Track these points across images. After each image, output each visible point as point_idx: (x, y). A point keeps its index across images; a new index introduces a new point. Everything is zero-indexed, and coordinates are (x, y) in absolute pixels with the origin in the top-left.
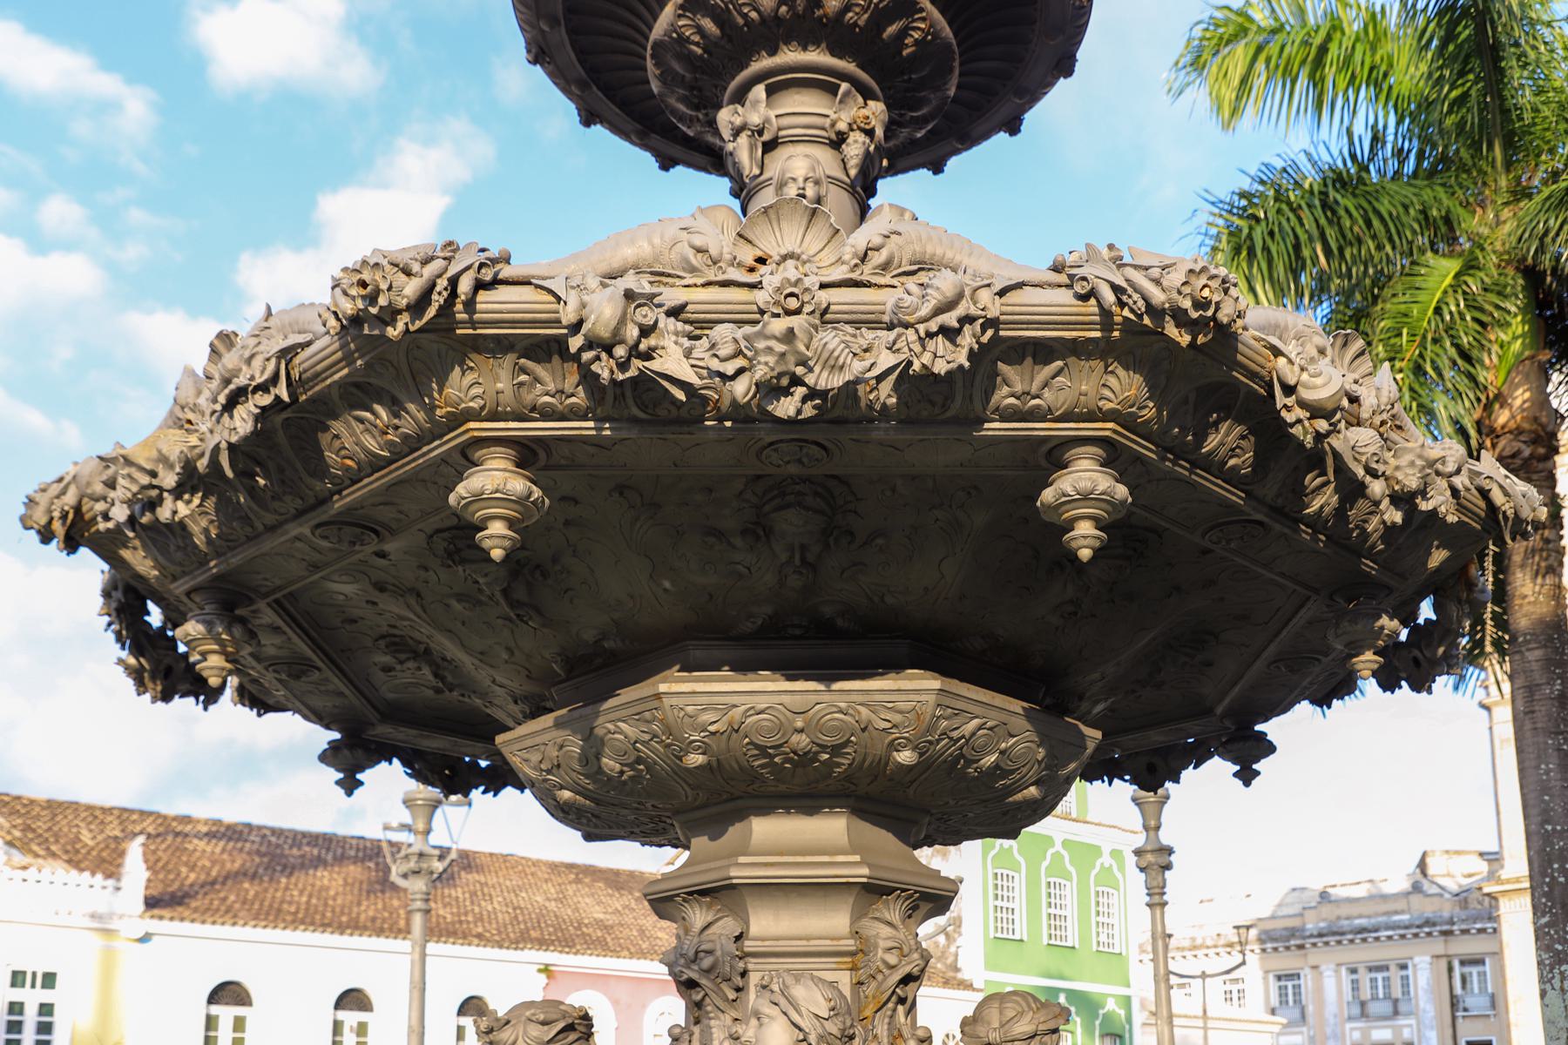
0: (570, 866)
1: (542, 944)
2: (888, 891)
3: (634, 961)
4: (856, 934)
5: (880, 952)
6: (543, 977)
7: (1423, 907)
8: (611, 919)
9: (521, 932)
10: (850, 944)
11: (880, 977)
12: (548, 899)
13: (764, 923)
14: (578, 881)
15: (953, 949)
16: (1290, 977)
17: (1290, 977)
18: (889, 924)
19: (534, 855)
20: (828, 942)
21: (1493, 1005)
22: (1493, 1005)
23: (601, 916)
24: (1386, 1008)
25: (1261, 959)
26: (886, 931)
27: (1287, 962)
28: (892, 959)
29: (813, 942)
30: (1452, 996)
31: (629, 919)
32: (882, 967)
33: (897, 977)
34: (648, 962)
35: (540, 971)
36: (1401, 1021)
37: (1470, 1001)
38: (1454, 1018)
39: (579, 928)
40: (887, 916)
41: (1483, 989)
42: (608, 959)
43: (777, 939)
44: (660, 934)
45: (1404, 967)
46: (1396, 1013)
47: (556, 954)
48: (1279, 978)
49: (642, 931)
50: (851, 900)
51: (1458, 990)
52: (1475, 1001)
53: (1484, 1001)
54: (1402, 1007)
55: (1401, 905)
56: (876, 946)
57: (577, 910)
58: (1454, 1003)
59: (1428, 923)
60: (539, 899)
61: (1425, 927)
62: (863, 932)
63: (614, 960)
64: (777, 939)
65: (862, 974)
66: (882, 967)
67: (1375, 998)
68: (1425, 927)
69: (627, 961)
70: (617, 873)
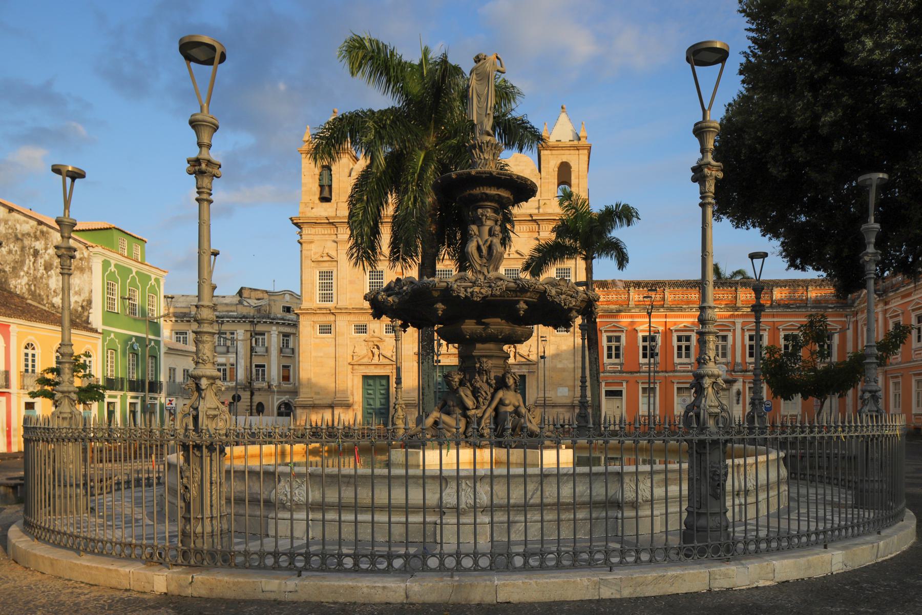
7: (243, 310)
15: (86, 314)
16: (182, 333)
17: (182, 333)
21: (267, 351)
22: (267, 351)
24: (224, 349)
25: (173, 325)
27: (182, 327)
30: (251, 347)
36: (230, 355)
37: (258, 349)
38: (251, 355)
41: (263, 345)
45: (233, 334)
46: (228, 352)
48: (177, 333)
51: (254, 345)
52: (260, 349)
53: (263, 349)
54: (231, 350)
55: (234, 308)
58: (252, 349)
59: (244, 317)
61: (242, 319)
67: (219, 345)
68: (242, 319)
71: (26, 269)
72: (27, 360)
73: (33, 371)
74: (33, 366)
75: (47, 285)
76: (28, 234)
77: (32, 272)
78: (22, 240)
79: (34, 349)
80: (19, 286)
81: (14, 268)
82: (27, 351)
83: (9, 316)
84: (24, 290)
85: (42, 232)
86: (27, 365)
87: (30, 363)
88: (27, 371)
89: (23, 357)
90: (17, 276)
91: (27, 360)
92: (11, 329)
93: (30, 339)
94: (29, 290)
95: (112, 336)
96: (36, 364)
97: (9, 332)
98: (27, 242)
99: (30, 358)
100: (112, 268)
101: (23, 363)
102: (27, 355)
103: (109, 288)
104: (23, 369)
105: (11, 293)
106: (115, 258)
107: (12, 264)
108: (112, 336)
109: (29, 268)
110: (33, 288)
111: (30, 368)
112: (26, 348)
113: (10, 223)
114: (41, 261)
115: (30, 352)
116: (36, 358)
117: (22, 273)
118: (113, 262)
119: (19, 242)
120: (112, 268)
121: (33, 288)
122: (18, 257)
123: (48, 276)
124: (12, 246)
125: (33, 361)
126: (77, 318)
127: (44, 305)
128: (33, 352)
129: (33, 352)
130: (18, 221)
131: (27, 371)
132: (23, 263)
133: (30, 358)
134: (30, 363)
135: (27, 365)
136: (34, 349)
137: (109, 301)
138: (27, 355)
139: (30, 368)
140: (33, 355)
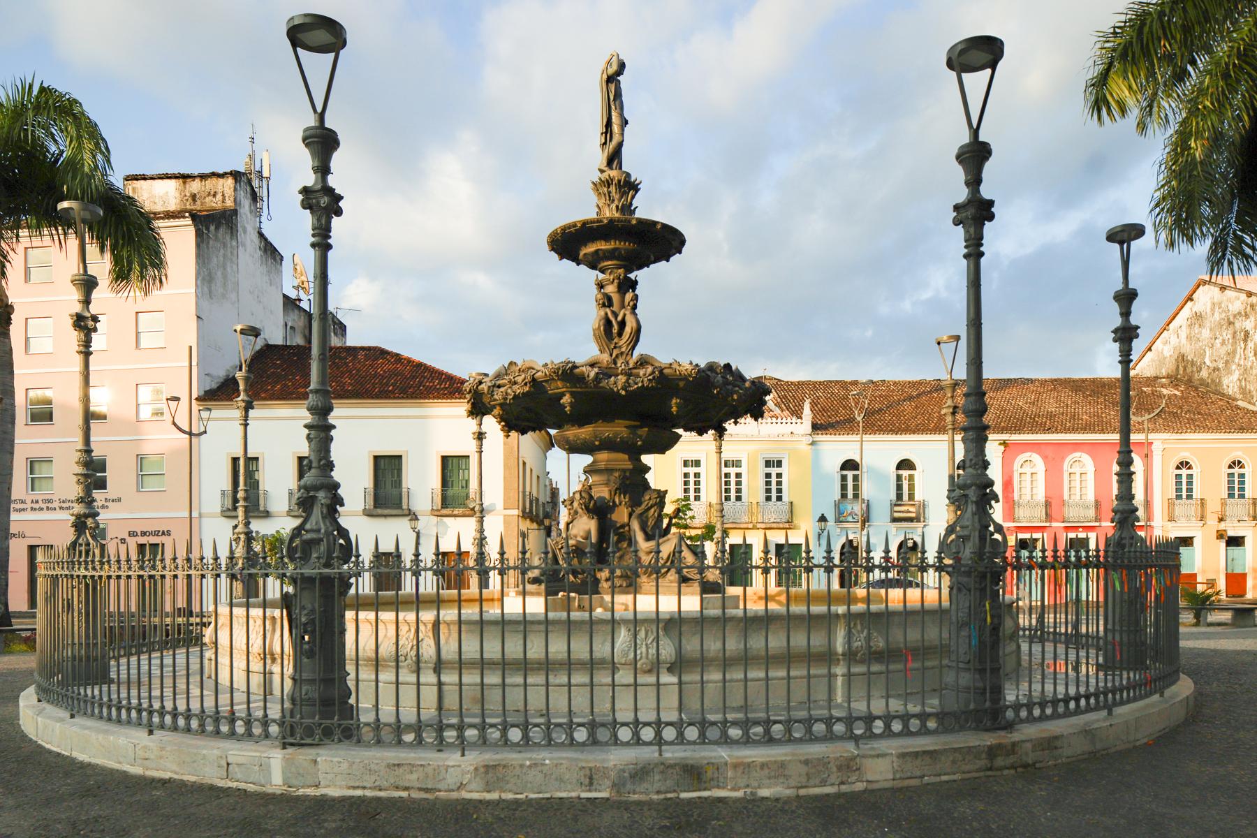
1: (1002, 430)
6: (1002, 448)
76: (1239, 313)
81: (1227, 362)
84: (1236, 389)
90: (1230, 373)
93: (1185, 456)
94: (1240, 387)
98: (1238, 325)
105: (1223, 395)
117: (1234, 367)
128: (1189, 472)
130: (1229, 300)
132: (1234, 352)
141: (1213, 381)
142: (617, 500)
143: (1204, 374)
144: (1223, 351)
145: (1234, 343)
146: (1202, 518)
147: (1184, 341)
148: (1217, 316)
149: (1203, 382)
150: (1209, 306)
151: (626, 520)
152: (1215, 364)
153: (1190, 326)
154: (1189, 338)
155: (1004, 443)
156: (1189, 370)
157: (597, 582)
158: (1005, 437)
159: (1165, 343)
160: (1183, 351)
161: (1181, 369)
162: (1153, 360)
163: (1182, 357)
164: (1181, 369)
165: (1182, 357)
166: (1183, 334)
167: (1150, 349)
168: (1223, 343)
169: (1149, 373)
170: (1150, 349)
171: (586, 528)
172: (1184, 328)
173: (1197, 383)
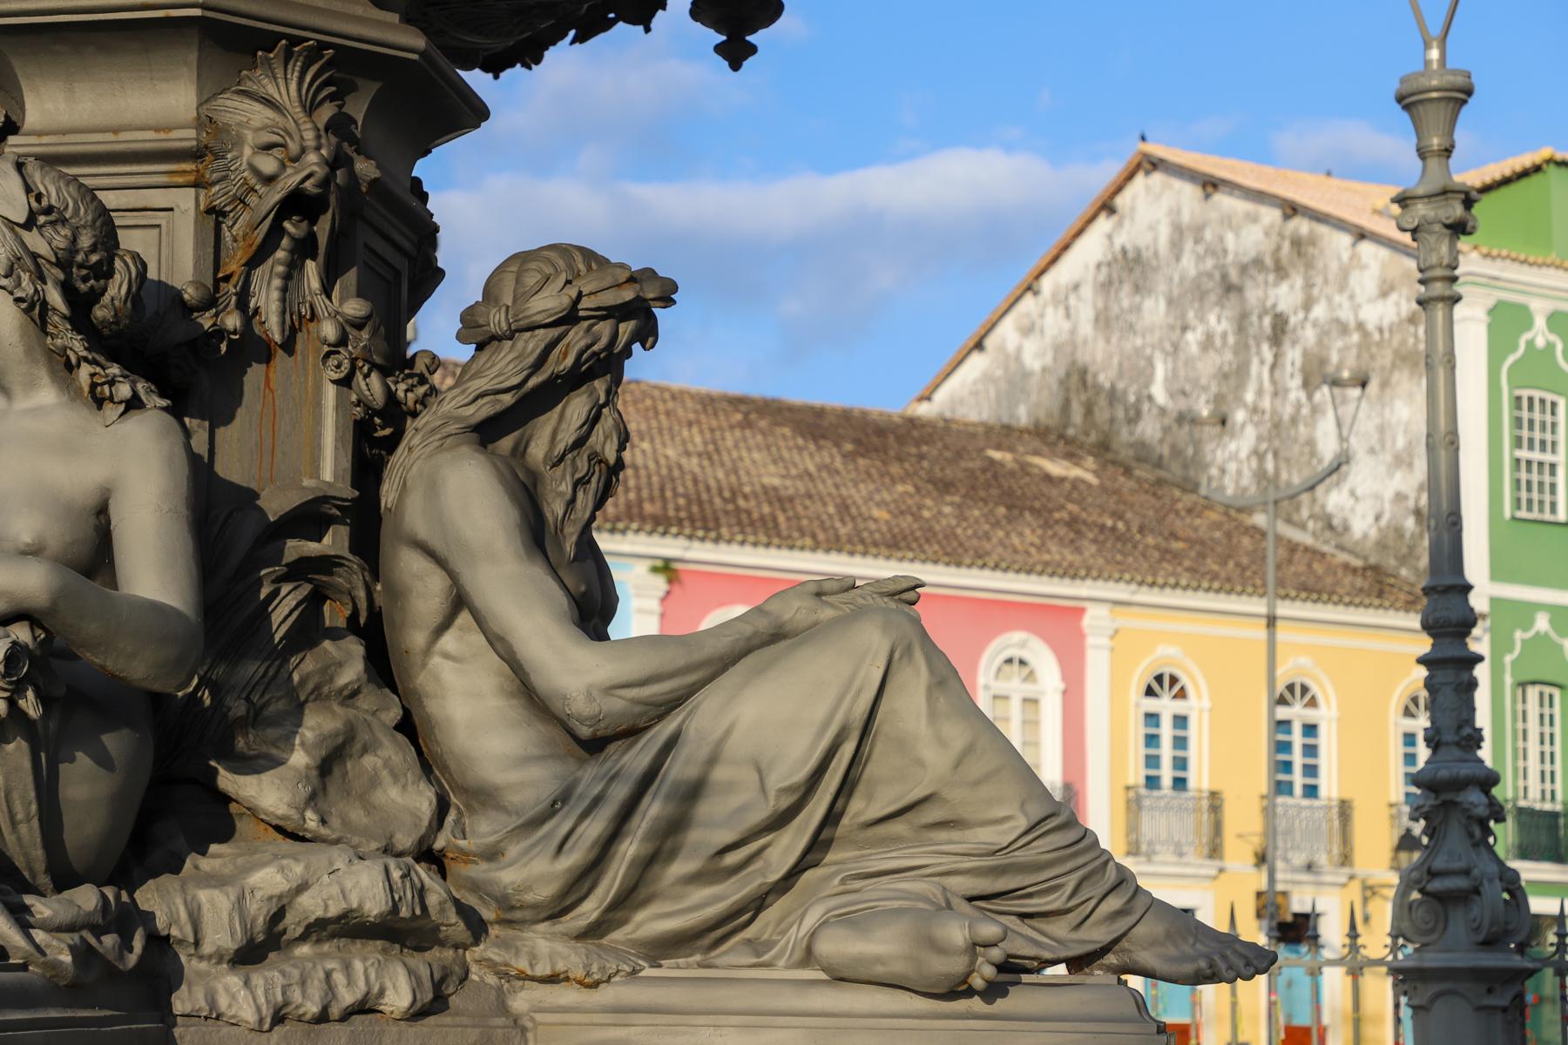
0: (737, 402)
1: (661, 524)
2: (268, 41)
3: (820, 555)
4: (205, 122)
5: (247, 151)
6: (660, 583)
8: (790, 487)
9: (629, 505)
10: (186, 137)
11: (252, 200)
12: (688, 454)
13: (49, 106)
14: (746, 424)
18: (268, 102)
19: (677, 384)
20: (150, 135)
23: (776, 482)
26: (259, 114)
28: (268, 165)
29: (124, 136)
31: (826, 486)
32: (253, 181)
33: (275, 195)
34: (844, 558)
35: (655, 570)
39: (733, 500)
40: (271, 90)
42: (773, 551)
43: (64, 132)
44: (876, 513)
47: (682, 541)
49: (844, 508)
50: (193, 57)
56: (239, 142)
57: (736, 471)
60: (670, 452)
62: (223, 118)
63: (785, 553)
64: (64, 132)
65: (218, 195)
66: (253, 181)
69: (807, 555)
70: (820, 412)
71: (1249, 397)
72: (1152, 740)
73: (1180, 783)
74: (1181, 763)
75: (1311, 443)
76: (1258, 262)
77: (1266, 403)
78: (1239, 289)
79: (1182, 694)
80: (1232, 467)
82: (1151, 704)
83: (1070, 573)
84: (1247, 480)
85: (1297, 243)
86: (1152, 761)
87: (1166, 751)
88: (1152, 782)
89: (1136, 731)
91: (1152, 740)
92: (1086, 622)
93: (1166, 655)
94: (1260, 475)
95: (1542, 623)
96: (1192, 753)
97: (1081, 636)
98: (1253, 295)
99: (1166, 731)
100: (1540, 334)
101: (1136, 751)
102: (1152, 718)
103: (1526, 422)
104: (1136, 774)
106: (1545, 289)
107: (1214, 389)
108: (1542, 623)
109: (1260, 393)
110: (1270, 466)
111: (1167, 774)
112: (1150, 692)
113: (1208, 235)
114: (1293, 356)
115: (1165, 706)
116: (1192, 732)
117: (1240, 416)
118: (1539, 309)
119: (1233, 296)
120: (1540, 334)
121: (1270, 466)
122: (1229, 356)
123: (1316, 410)
124: (1212, 318)
125: (1180, 742)
126: (1403, 560)
127: (1302, 526)
128: (1179, 707)
129: (1179, 707)
130: (1228, 221)
131: (1152, 782)
133: (1166, 731)
134: (1166, 751)
135: (1152, 761)
136: (1182, 694)
137: (1529, 482)
138: (1152, 718)
139: (1167, 774)
140: (1181, 721)
141: (1176, 452)
142: (267, 298)
143: (1149, 428)
144: (1207, 367)
145: (1242, 348)
146: (1215, 850)
147: (1086, 329)
148: (1189, 265)
149: (1143, 452)
150: (1164, 233)
151: (330, 468)
152: (1182, 404)
153: (1106, 287)
154: (1103, 321)
155: (666, 568)
156: (1102, 415)
157: (160, 969)
158: (671, 547)
159: (1028, 330)
160: (1083, 357)
161: (1077, 416)
162: (987, 378)
163: (1077, 378)
164: (1077, 416)
165: (1077, 378)
166: (1085, 311)
167: (979, 346)
168: (1207, 343)
169: (976, 413)
170: (979, 346)
171: (78, 477)
172: (1087, 291)
173: (1126, 454)
